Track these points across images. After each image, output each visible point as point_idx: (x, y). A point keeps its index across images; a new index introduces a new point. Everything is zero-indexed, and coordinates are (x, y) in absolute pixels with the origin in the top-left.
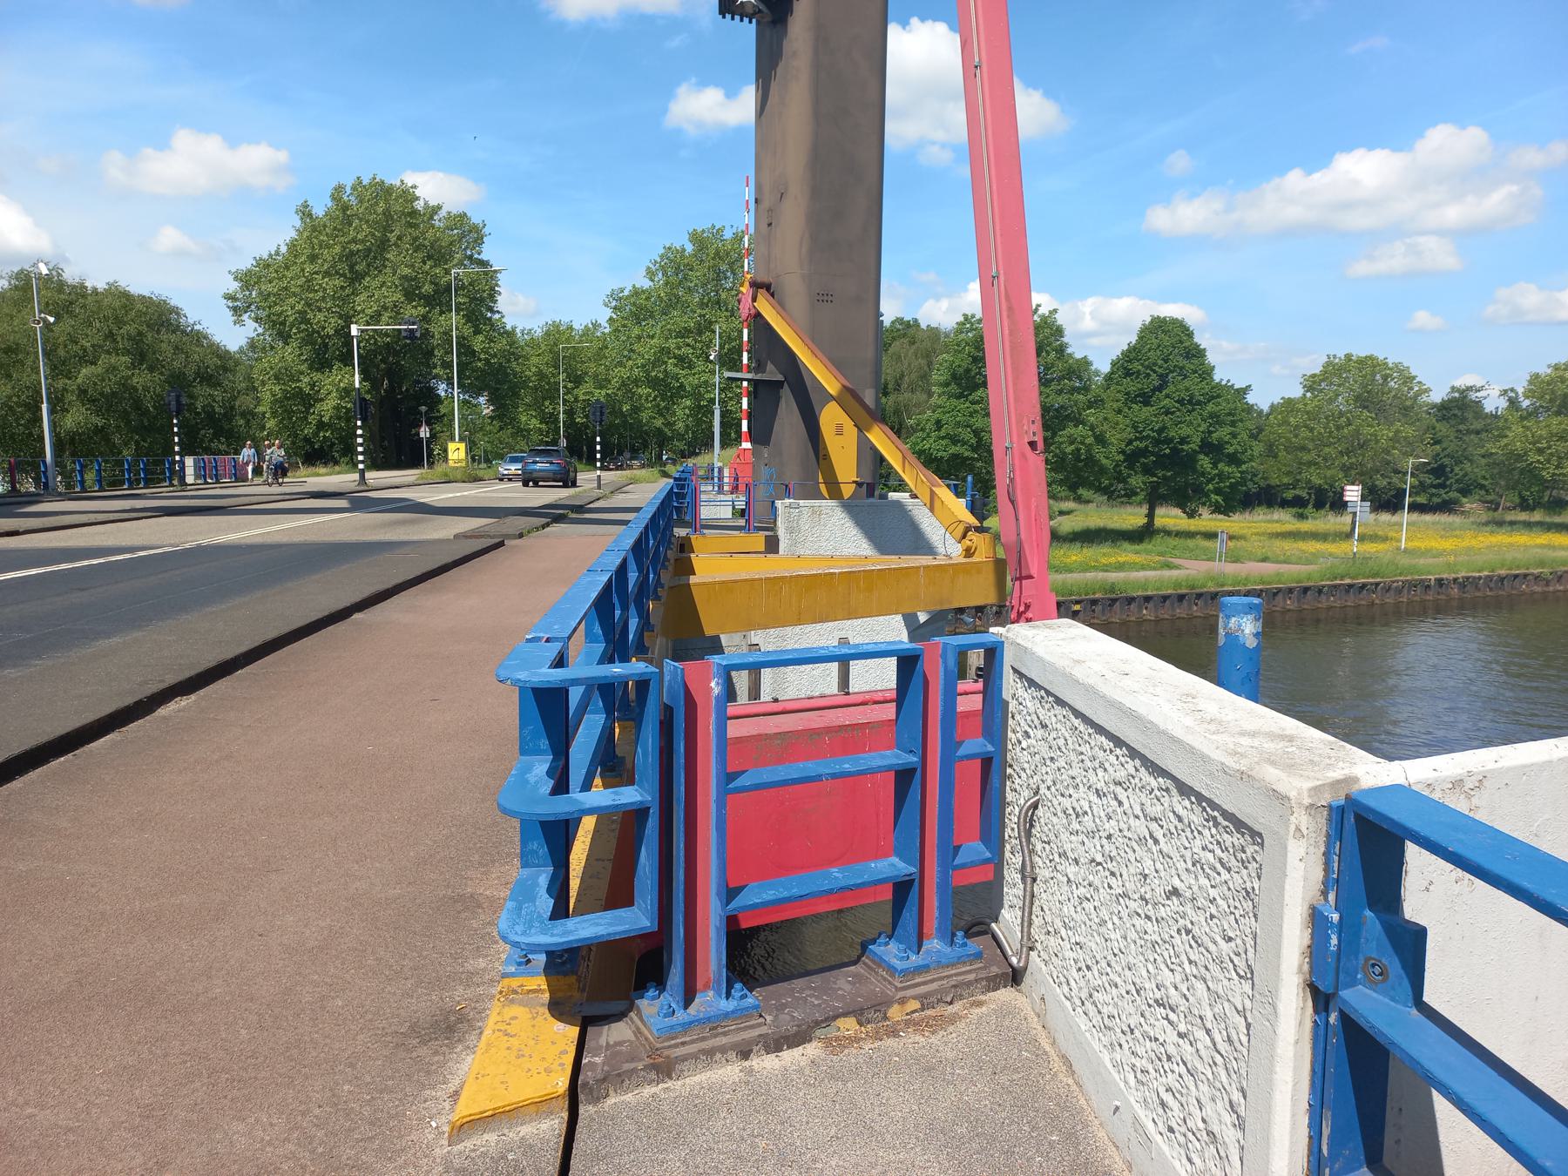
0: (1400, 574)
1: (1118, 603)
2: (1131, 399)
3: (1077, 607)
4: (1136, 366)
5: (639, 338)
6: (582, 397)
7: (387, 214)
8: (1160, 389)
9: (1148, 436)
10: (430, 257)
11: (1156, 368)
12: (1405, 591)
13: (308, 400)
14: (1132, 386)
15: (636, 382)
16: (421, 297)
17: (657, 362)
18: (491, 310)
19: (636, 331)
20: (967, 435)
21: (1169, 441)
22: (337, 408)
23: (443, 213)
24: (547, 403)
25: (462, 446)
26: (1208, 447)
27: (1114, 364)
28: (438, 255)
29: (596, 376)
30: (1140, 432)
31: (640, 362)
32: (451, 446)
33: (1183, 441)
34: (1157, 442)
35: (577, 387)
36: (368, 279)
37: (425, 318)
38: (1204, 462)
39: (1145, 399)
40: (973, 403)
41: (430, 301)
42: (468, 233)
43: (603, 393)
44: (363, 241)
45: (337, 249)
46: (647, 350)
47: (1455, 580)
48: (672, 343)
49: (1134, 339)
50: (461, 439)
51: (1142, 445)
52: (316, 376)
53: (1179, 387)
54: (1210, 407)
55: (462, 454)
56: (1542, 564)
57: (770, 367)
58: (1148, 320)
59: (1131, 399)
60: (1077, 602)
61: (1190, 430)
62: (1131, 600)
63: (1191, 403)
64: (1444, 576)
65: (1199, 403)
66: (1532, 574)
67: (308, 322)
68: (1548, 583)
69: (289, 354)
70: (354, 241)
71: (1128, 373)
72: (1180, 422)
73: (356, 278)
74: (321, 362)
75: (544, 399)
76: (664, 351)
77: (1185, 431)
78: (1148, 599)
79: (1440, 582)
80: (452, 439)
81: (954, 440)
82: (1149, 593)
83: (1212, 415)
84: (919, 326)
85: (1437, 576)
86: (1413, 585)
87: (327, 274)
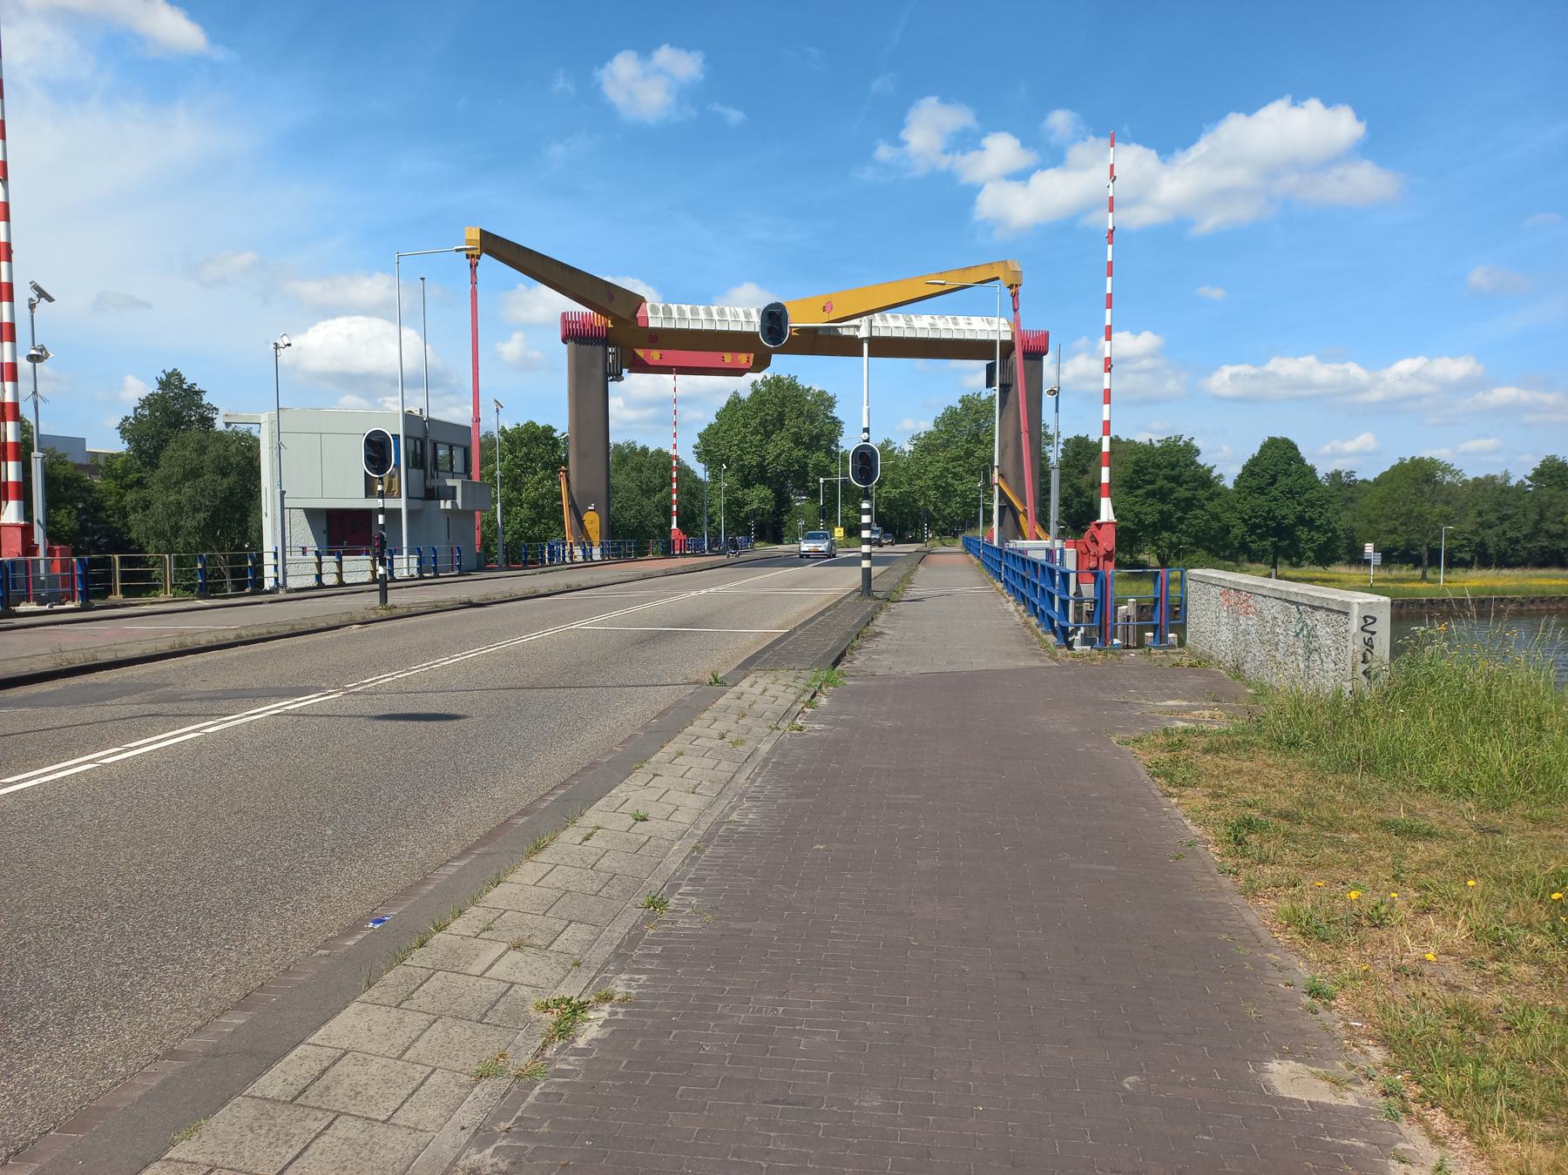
0: (1401, 596)
2: (1252, 491)
3: (1178, 609)
4: (1257, 470)
5: (931, 463)
6: (883, 495)
7: (784, 397)
8: (1272, 484)
9: (1261, 515)
11: (1269, 471)
12: (1405, 606)
14: (1254, 483)
15: (929, 488)
16: (804, 443)
17: (941, 476)
18: (837, 446)
19: (929, 459)
20: (1130, 515)
21: (1274, 518)
25: (842, 529)
26: (1301, 520)
27: (1244, 468)
29: (893, 479)
30: (1256, 513)
31: (931, 476)
32: (836, 529)
33: (1284, 518)
34: (1265, 519)
35: (880, 488)
36: (774, 436)
38: (1303, 533)
39: (1261, 490)
40: (1136, 496)
41: (808, 447)
42: (827, 401)
43: (898, 491)
46: (936, 470)
47: (1443, 601)
48: (950, 466)
49: (1256, 450)
50: (841, 526)
51: (1257, 521)
52: (746, 491)
53: (1283, 482)
54: (1307, 496)
55: (842, 534)
56: (1518, 593)
57: (1003, 501)
58: (1267, 439)
59: (1252, 491)
61: (1288, 511)
63: (1291, 493)
64: (1434, 598)
65: (1297, 493)
66: (1507, 598)
67: (742, 460)
68: (1522, 604)
70: (766, 414)
71: (1252, 474)
72: (1283, 506)
73: (768, 435)
74: (747, 484)
76: (947, 470)
77: (1285, 511)
79: (1431, 601)
80: (837, 526)
83: (1307, 500)
84: (1120, 440)
85: (1429, 598)
86: (1413, 603)
87: (752, 434)
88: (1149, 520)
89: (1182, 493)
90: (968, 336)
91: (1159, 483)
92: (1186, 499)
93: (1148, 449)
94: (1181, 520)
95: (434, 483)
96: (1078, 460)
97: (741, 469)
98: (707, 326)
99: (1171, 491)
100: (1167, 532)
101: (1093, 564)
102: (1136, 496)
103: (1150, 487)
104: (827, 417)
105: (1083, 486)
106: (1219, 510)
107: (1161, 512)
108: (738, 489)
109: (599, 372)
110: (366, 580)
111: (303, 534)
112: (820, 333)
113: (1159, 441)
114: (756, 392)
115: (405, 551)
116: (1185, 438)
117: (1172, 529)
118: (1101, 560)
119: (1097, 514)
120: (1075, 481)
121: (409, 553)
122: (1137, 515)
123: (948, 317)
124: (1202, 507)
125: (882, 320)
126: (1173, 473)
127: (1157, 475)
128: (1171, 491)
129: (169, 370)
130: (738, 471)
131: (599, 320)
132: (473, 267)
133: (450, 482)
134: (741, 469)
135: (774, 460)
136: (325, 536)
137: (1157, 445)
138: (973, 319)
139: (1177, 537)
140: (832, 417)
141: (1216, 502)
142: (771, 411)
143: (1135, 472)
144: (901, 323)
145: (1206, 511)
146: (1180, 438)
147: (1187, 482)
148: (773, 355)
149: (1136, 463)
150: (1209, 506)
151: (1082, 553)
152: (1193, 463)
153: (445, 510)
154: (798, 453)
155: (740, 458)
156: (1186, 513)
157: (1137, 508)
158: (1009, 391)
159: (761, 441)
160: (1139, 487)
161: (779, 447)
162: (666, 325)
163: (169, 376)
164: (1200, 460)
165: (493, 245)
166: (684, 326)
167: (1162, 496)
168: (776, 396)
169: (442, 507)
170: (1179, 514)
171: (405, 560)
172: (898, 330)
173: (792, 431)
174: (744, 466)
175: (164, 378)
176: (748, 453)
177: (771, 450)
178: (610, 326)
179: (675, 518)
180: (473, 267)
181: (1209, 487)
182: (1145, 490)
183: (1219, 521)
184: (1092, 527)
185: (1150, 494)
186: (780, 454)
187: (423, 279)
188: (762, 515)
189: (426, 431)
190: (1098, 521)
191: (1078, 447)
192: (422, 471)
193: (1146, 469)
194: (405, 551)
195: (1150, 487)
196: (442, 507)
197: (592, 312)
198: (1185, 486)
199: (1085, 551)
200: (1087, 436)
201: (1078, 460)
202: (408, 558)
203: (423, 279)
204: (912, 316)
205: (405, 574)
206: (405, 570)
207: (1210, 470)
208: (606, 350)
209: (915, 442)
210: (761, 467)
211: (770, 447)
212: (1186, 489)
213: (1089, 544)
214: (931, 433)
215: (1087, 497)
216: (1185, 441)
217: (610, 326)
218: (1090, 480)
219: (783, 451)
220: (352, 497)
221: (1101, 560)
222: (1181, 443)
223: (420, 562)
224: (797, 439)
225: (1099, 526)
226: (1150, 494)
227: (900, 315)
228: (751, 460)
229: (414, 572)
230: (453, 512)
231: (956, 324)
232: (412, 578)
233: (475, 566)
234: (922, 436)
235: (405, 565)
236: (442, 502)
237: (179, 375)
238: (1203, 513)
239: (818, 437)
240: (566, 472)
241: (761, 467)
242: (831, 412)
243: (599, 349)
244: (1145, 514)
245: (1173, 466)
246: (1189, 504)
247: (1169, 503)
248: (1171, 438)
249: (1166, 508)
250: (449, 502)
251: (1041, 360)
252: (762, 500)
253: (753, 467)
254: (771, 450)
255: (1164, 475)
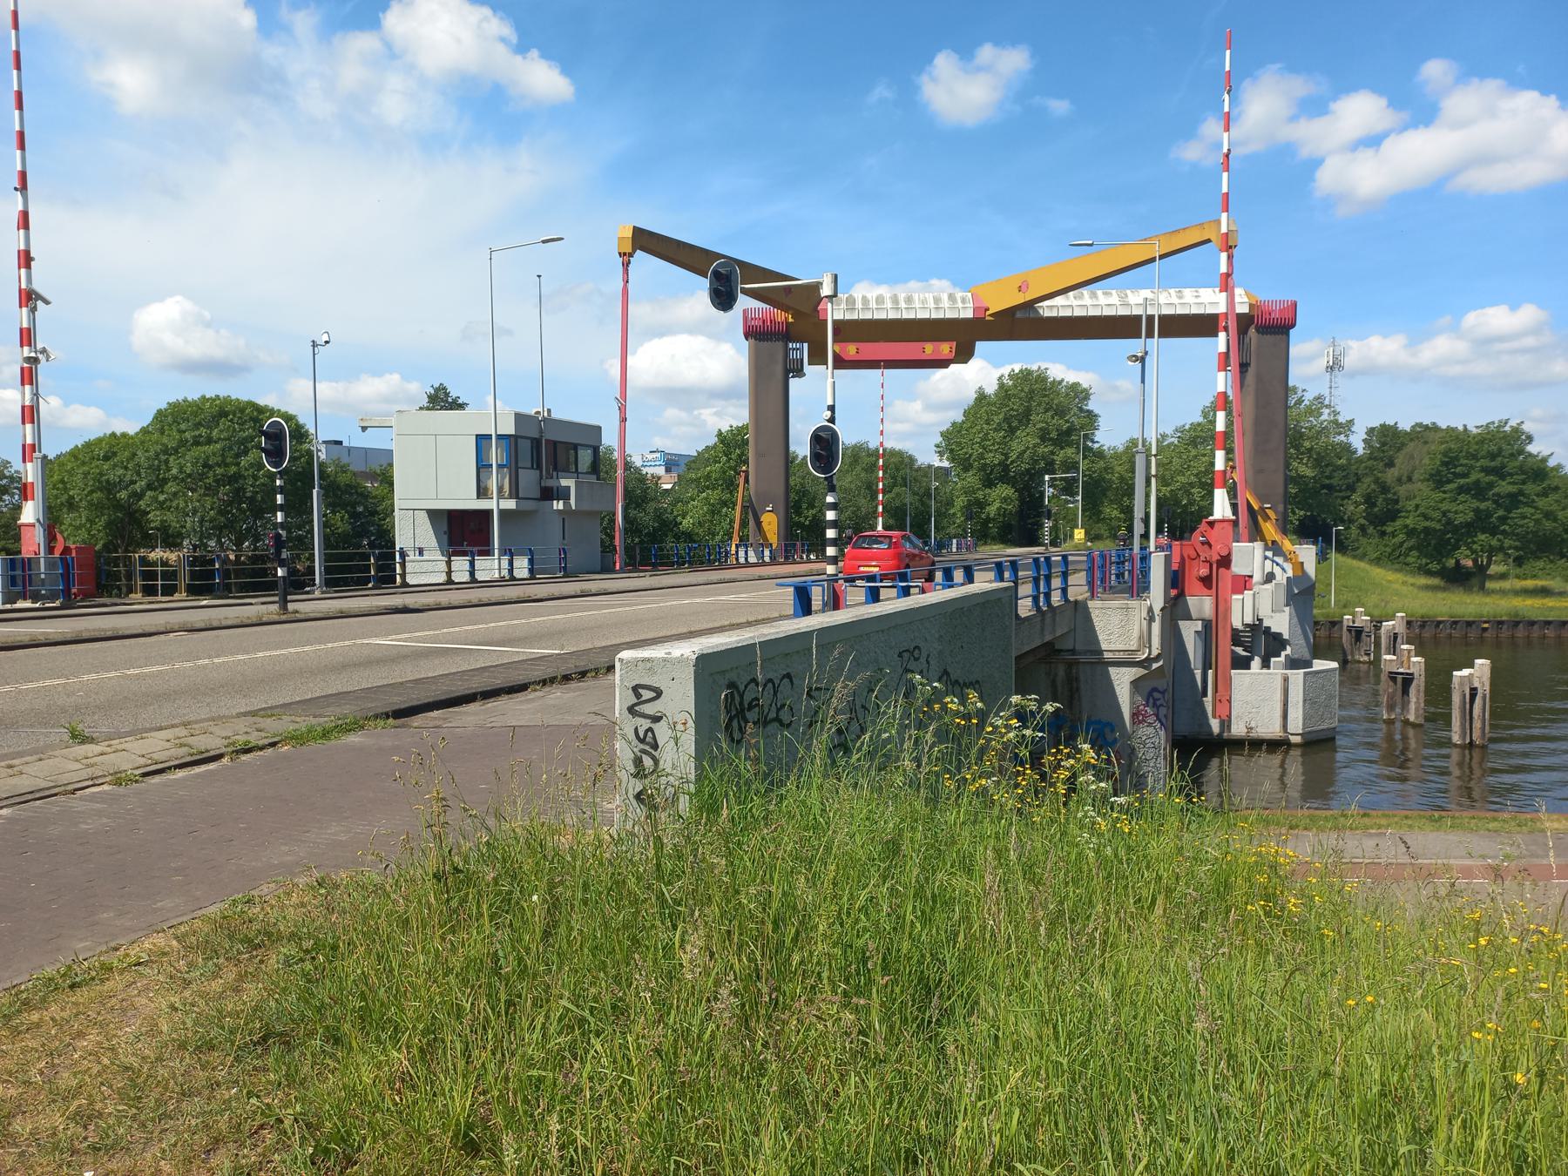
1: (1521, 625)
3: (1486, 625)
5: (1195, 457)
7: (1032, 391)
10: (1056, 414)
13: (982, 505)
15: (1192, 485)
16: (1051, 439)
19: (1193, 452)
20: (1436, 515)
22: (999, 509)
23: (1064, 383)
24: (1125, 499)
25: (1083, 531)
28: (1061, 412)
32: (1076, 531)
37: (1052, 453)
41: (1056, 442)
42: (1079, 394)
43: (1169, 489)
44: (1017, 411)
45: (1001, 416)
52: (988, 491)
55: (1083, 536)
60: (1485, 622)
62: (1532, 623)
69: (972, 479)
70: (1012, 409)
74: (989, 483)
75: (1123, 496)
78: (1548, 623)
80: (1077, 527)
81: (1426, 517)
82: (1550, 619)
87: (995, 430)
88: (1460, 519)
89: (1504, 487)
90: (1195, 310)
91: (1474, 477)
92: (1511, 496)
93: (1455, 436)
94: (1503, 519)
95: (550, 483)
96: (1383, 452)
97: (983, 468)
98: (892, 315)
99: (1491, 485)
100: (1483, 533)
101: (1204, 572)
102: (1444, 492)
103: (1462, 481)
104: (1081, 409)
105: (1389, 481)
106: (1555, 507)
107: (1477, 511)
108: (978, 489)
109: (779, 369)
110: (441, 581)
111: (426, 535)
112: (1019, 315)
113: (1477, 427)
114: (1002, 386)
115: (496, 551)
116: (1513, 423)
117: (1493, 531)
118: (1215, 566)
119: (1210, 510)
120: (1380, 475)
121: (501, 554)
122: (1444, 514)
123: (1172, 291)
124: (1531, 504)
125: (1091, 298)
126: (1493, 464)
127: (1472, 467)
128: (1491, 485)
129: (436, 385)
130: (979, 470)
131: (780, 316)
132: (626, 265)
133: (564, 482)
134: (983, 468)
135: (1018, 457)
136: (446, 537)
137: (1475, 431)
138: (1202, 291)
139: (1499, 540)
140: (1088, 411)
141: (1553, 497)
142: (1015, 404)
143: (1444, 464)
144: (1114, 299)
145: (1536, 508)
146: (1506, 423)
147: (1511, 475)
148: (978, 344)
149: (1445, 454)
150: (1542, 503)
151: (1189, 556)
152: (1521, 452)
153: (558, 511)
154: (1044, 450)
155: (981, 456)
156: (1510, 512)
157: (1445, 506)
158: (1247, 371)
159: (1005, 437)
160: (1449, 482)
161: (1025, 442)
162: (848, 317)
163: (437, 390)
164: (1532, 448)
165: (645, 241)
166: (868, 316)
167: (1479, 491)
168: (1022, 390)
169: (555, 508)
170: (1501, 513)
171: (496, 561)
172: (1109, 308)
173: (1037, 426)
174: (985, 464)
175: (433, 392)
176: (991, 451)
177: (1016, 447)
178: (790, 320)
179: (880, 519)
180: (626, 265)
181: (1543, 480)
182: (1456, 485)
183: (1555, 520)
184: (1203, 527)
185: (1461, 490)
186: (1025, 451)
187: (539, 276)
188: (1004, 516)
189: (541, 431)
190: (1211, 518)
191: (1385, 436)
192: (538, 472)
193: (1458, 460)
194: (496, 551)
195: (1462, 481)
196: (555, 508)
197: (768, 307)
198: (1509, 479)
199: (1194, 555)
200: (1396, 424)
201: (1383, 452)
202: (499, 559)
203: (539, 276)
204: (1128, 292)
205: (497, 576)
206: (497, 571)
207: (1544, 460)
208: (787, 346)
209: (1179, 434)
210: (1005, 467)
211: (1014, 444)
212: (1510, 483)
213: (1199, 548)
214: (1199, 424)
215: (1395, 494)
216: (1511, 427)
217: (790, 320)
218: (1396, 474)
219: (1028, 448)
220: (464, 498)
221: (1215, 566)
222: (1507, 428)
223: (531, 561)
224: (1044, 436)
225: (1212, 524)
226: (1461, 490)
227: (1114, 292)
228: (993, 458)
229: (505, 573)
230: (567, 512)
231: (1180, 298)
232: (502, 579)
233: (599, 568)
234: (1187, 427)
235: (497, 567)
236: (555, 502)
237: (445, 389)
238: (1533, 511)
239: (1069, 432)
240: (746, 472)
241: (1005, 467)
242: (1086, 405)
243: (780, 344)
244: (1456, 512)
245: (1493, 456)
246: (1514, 500)
247: (1488, 499)
248: (1493, 423)
249: (1483, 506)
250: (561, 502)
251: (1288, 336)
252: (1004, 500)
253: (995, 465)
254: (1016, 447)
255: (1482, 466)
